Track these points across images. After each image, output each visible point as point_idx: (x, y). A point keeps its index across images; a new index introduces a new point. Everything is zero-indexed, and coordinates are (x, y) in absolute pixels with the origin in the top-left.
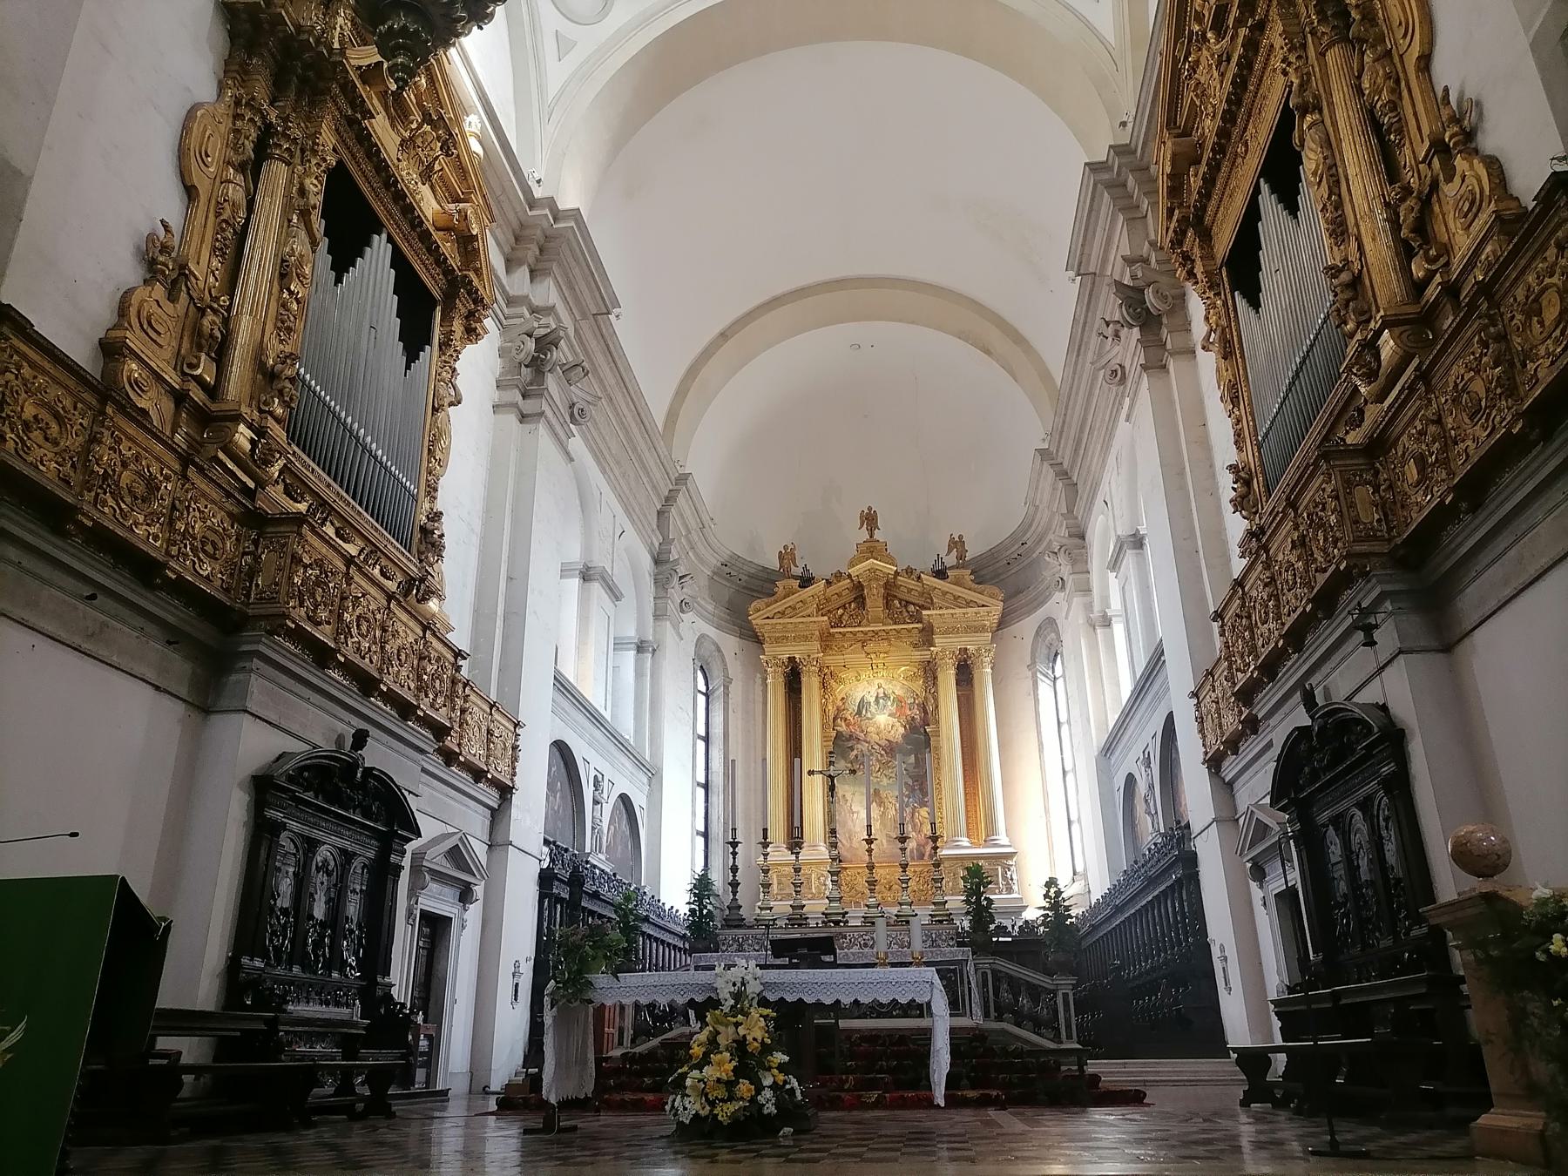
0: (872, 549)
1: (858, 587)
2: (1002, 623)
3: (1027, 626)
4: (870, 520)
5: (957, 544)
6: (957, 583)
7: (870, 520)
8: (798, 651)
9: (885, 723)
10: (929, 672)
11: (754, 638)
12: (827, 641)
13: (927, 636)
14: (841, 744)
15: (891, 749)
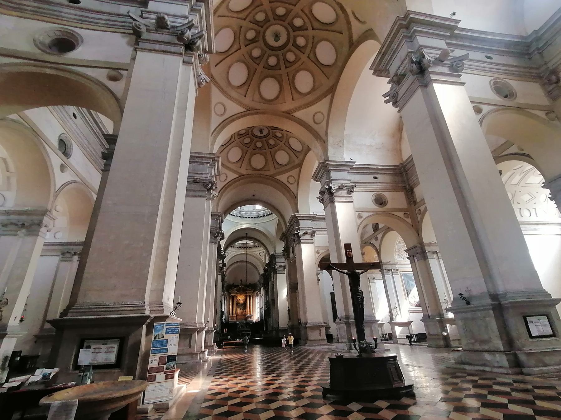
0: (241, 284)
1: (240, 288)
2: (254, 292)
3: (256, 292)
4: (241, 280)
5: (250, 283)
6: (250, 288)
7: (241, 280)
8: (234, 295)
9: (242, 302)
10: (246, 297)
11: (229, 294)
12: (236, 293)
13: (246, 293)
14: (238, 304)
15: (242, 304)
